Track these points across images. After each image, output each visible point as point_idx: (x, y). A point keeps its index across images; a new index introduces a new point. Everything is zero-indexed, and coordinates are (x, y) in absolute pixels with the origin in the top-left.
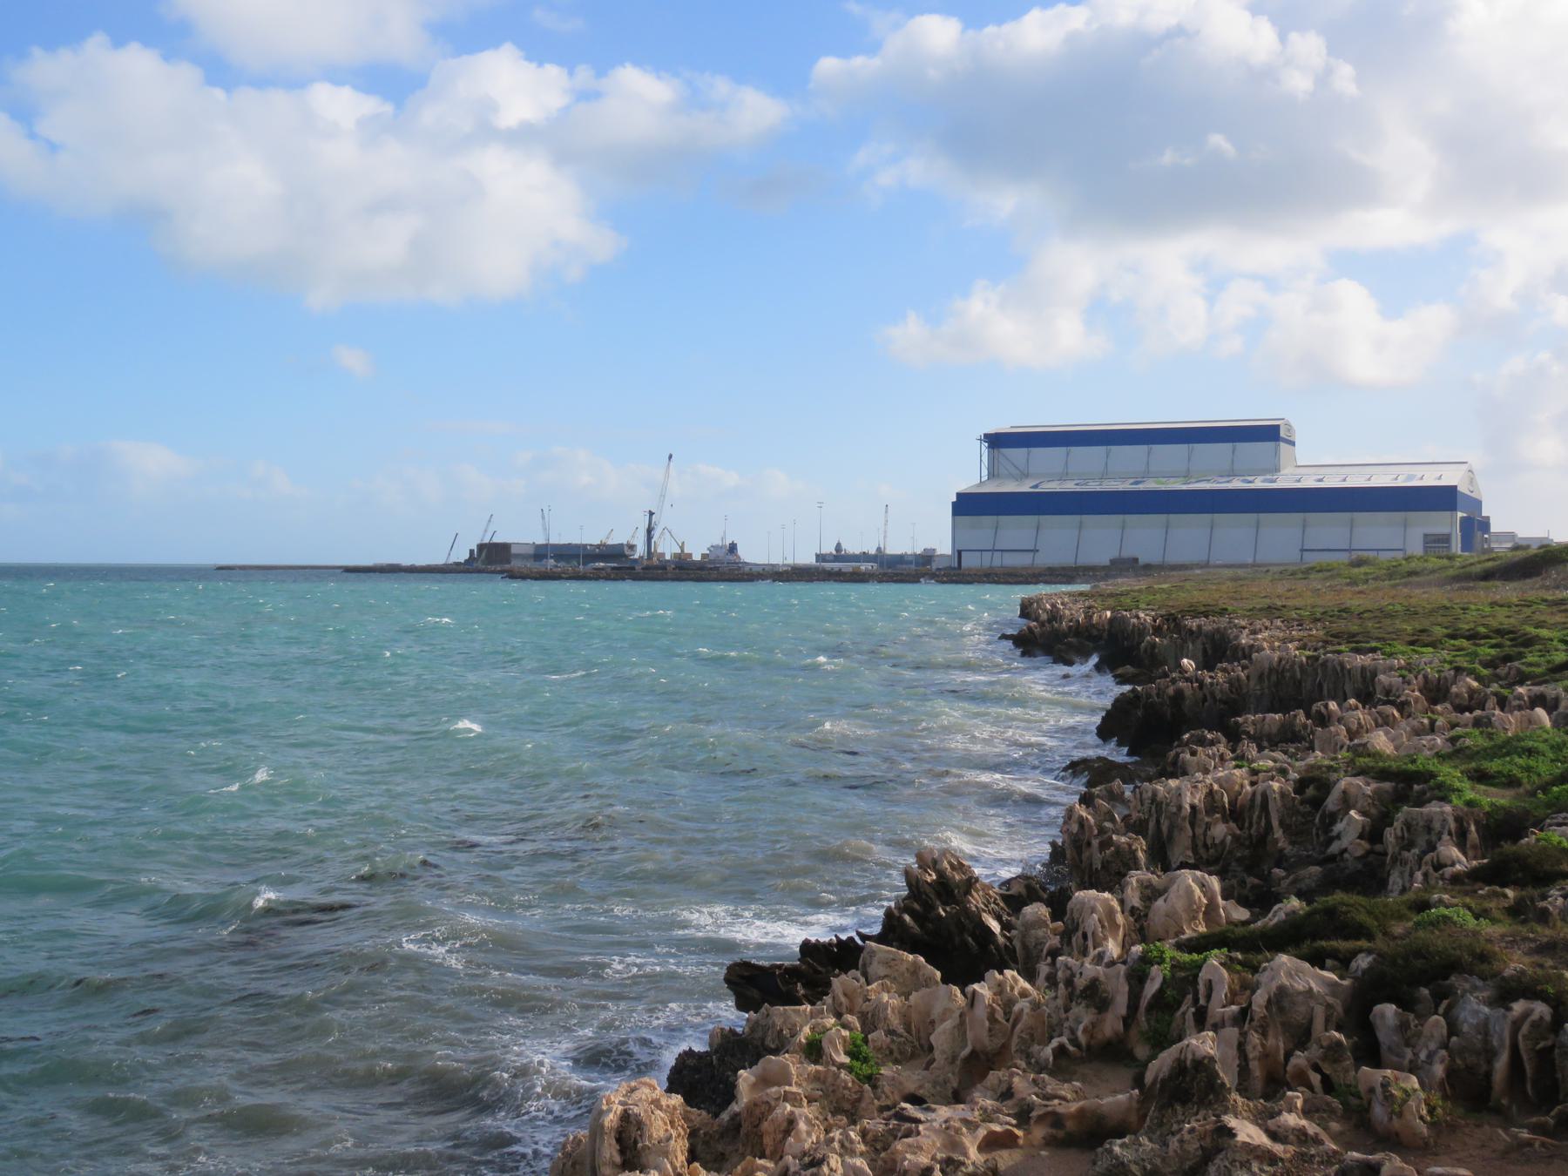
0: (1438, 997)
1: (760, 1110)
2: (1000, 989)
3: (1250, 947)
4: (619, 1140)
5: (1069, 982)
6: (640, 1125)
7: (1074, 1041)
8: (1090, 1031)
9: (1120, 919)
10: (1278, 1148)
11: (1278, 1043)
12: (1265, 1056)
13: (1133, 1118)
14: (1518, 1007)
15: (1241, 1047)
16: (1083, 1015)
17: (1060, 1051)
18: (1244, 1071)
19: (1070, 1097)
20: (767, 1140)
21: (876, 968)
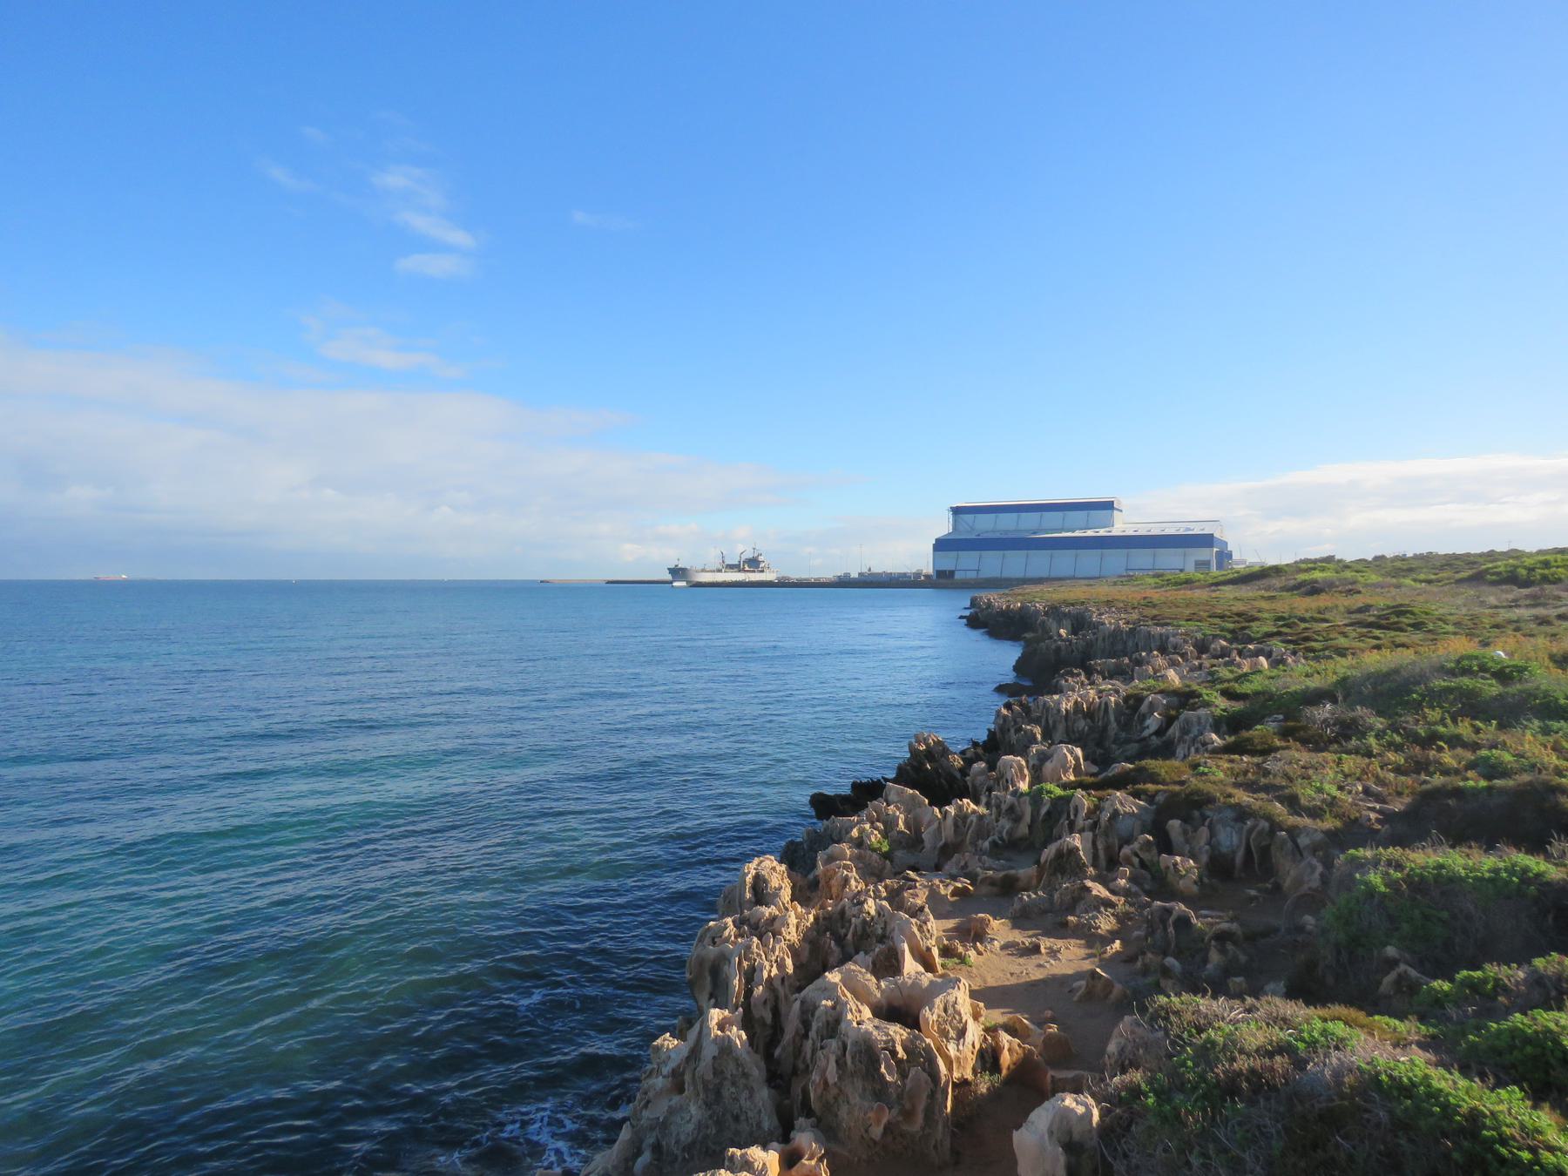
5: (998, 807)
6: (765, 881)
7: (1001, 838)
8: (1010, 833)
10: (1114, 898)
12: (1108, 848)
13: (1034, 882)
15: (1094, 843)
16: (1006, 824)
17: (994, 844)
18: (1095, 857)
20: (834, 890)
21: (893, 797)
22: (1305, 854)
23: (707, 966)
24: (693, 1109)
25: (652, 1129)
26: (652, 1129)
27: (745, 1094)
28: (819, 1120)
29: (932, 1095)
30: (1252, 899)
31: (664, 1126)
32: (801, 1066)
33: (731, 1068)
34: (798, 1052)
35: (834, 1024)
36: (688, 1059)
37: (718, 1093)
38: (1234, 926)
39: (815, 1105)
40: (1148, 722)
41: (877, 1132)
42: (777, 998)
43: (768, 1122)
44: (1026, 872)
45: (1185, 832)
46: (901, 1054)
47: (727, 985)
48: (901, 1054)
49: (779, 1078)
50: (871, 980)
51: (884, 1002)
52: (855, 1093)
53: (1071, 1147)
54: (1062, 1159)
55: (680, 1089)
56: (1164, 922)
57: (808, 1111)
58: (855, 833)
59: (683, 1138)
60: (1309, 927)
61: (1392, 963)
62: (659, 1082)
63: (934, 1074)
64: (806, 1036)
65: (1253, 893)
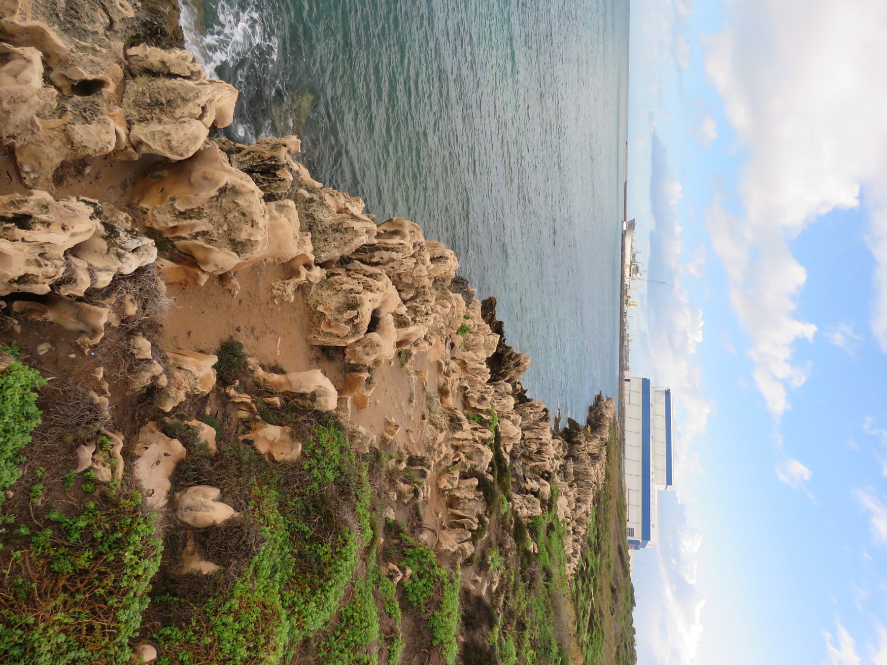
0: (479, 497)
1: (449, 299)
3: (496, 444)
5: (486, 392)
8: (472, 398)
11: (467, 450)
12: (463, 446)
14: (476, 520)
16: (477, 396)
17: (466, 388)
18: (459, 439)
21: (492, 338)
22: (460, 545)
23: (400, 229)
24: (330, 218)
25: (321, 198)
26: (321, 198)
27: (336, 244)
28: (325, 281)
29: (339, 337)
30: (437, 514)
31: (322, 203)
32: (350, 273)
33: (348, 237)
34: (356, 271)
35: (368, 288)
36: (352, 215)
38: (421, 498)
39: (332, 279)
40: (534, 482)
41: (320, 308)
42: (384, 264)
43: (324, 257)
44: (452, 401)
45: (472, 487)
46: (356, 321)
48: (356, 321)
49: (344, 261)
51: (381, 316)
53: (313, 397)
54: (309, 391)
55: (339, 212)
56: (423, 465)
59: (317, 213)
60: (421, 536)
61: (403, 570)
62: (342, 201)
64: (364, 275)
65: (440, 515)
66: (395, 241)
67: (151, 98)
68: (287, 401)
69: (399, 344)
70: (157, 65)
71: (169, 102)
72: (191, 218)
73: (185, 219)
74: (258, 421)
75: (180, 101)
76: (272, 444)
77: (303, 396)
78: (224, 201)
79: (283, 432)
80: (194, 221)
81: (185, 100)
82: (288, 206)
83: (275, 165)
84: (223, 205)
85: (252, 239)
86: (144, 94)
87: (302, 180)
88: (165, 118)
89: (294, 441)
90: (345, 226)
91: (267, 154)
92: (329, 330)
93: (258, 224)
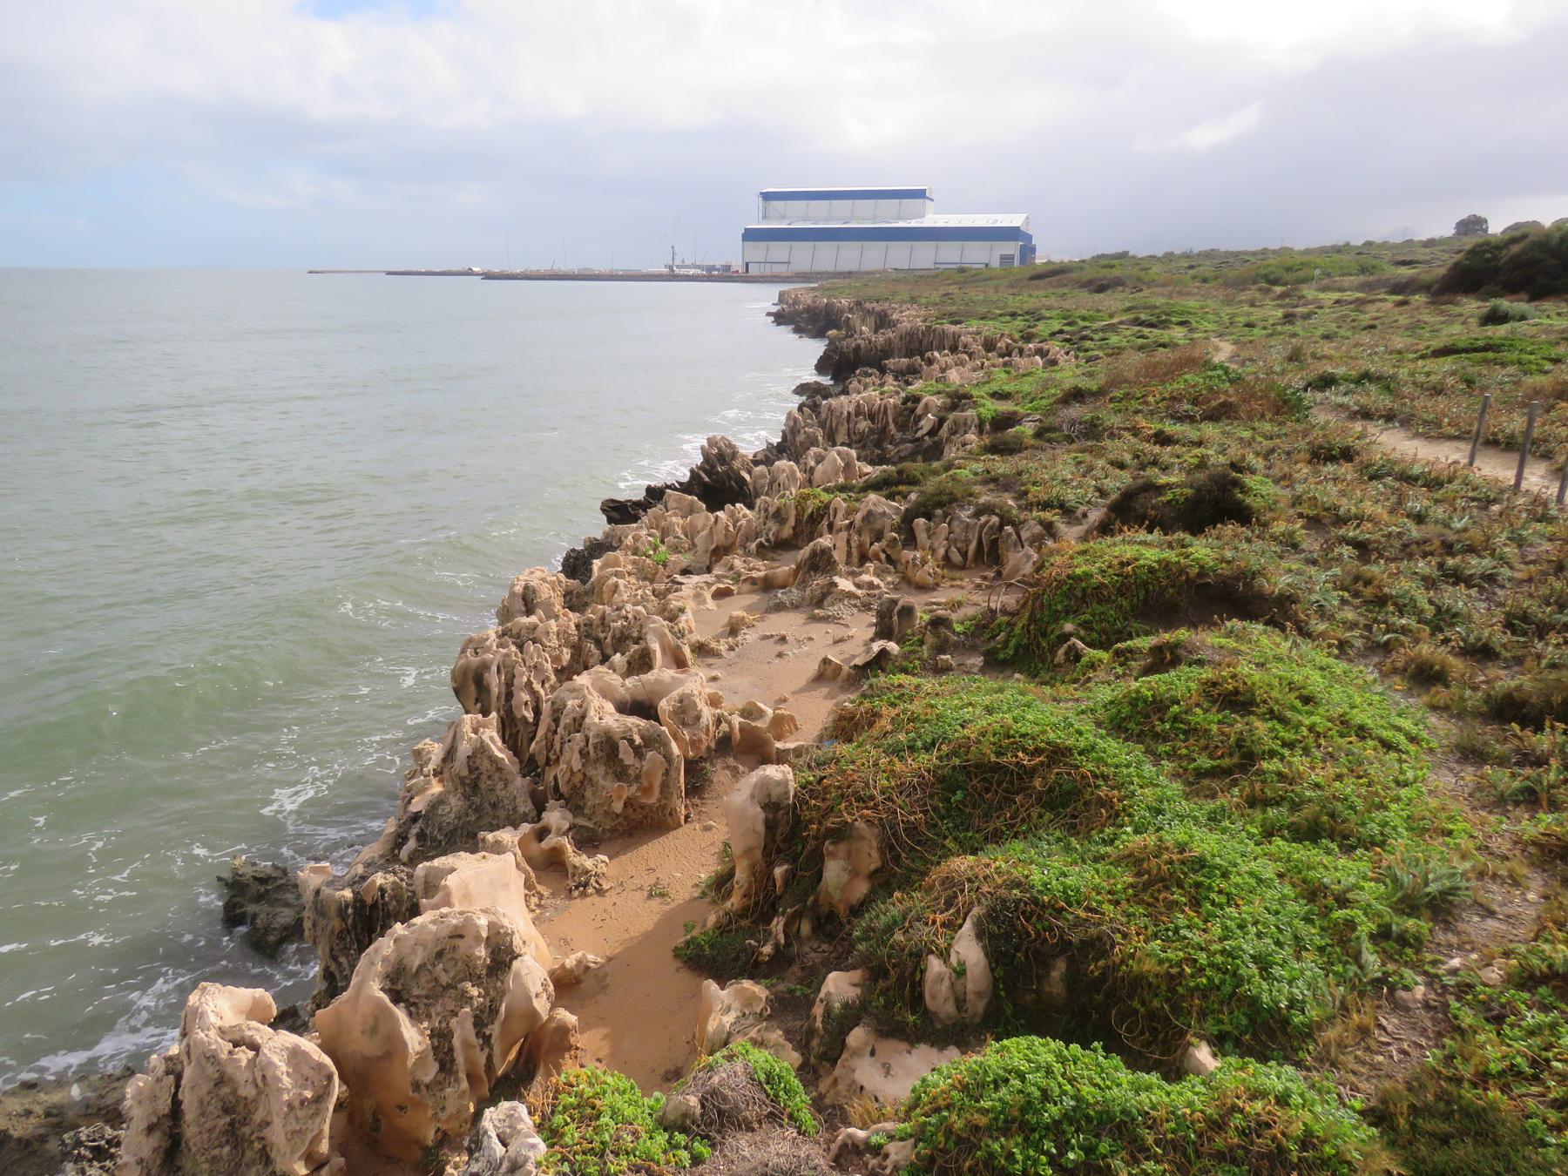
1: (602, 580)
2: (732, 515)
4: (524, 599)
5: (766, 510)
6: (534, 591)
7: (768, 540)
9: (799, 474)
10: (859, 592)
11: (866, 539)
12: (861, 546)
14: (983, 519)
15: (848, 541)
17: (761, 545)
18: (849, 554)
19: (760, 569)
21: (671, 504)
23: (471, 675)
27: (500, 785)
29: (667, 772)
33: (485, 765)
34: (550, 746)
35: (579, 722)
36: (444, 760)
37: (475, 787)
39: (563, 788)
40: (922, 423)
41: (618, 807)
43: (525, 806)
45: (928, 529)
46: (638, 740)
47: (488, 690)
48: (638, 740)
49: (530, 767)
50: (614, 679)
52: (598, 773)
54: (762, 816)
56: (890, 612)
57: (558, 795)
58: (629, 541)
63: (668, 757)
64: (555, 732)
66: (495, 682)
67: (221, 1146)
68: (779, 851)
69: (680, 663)
70: (155, 1140)
71: (226, 1110)
72: (451, 1049)
73: (453, 1061)
74: (816, 900)
75: (225, 1090)
76: (854, 874)
77: (770, 826)
78: (415, 992)
79: (833, 855)
80: (456, 1042)
81: (222, 1080)
82: (426, 876)
83: (354, 908)
84: (423, 993)
85: (485, 935)
86: (214, 1160)
87: (381, 856)
88: (257, 1117)
89: (850, 836)
90: (465, 772)
91: (336, 924)
92: (657, 790)
93: (456, 927)
